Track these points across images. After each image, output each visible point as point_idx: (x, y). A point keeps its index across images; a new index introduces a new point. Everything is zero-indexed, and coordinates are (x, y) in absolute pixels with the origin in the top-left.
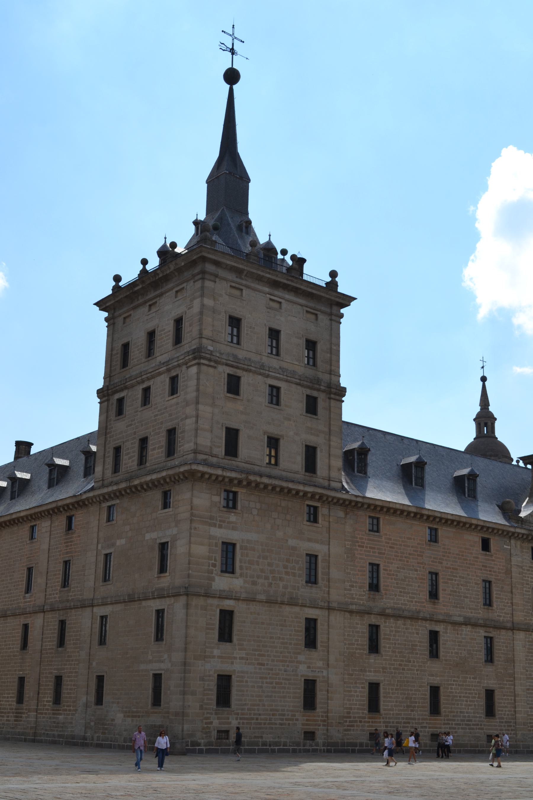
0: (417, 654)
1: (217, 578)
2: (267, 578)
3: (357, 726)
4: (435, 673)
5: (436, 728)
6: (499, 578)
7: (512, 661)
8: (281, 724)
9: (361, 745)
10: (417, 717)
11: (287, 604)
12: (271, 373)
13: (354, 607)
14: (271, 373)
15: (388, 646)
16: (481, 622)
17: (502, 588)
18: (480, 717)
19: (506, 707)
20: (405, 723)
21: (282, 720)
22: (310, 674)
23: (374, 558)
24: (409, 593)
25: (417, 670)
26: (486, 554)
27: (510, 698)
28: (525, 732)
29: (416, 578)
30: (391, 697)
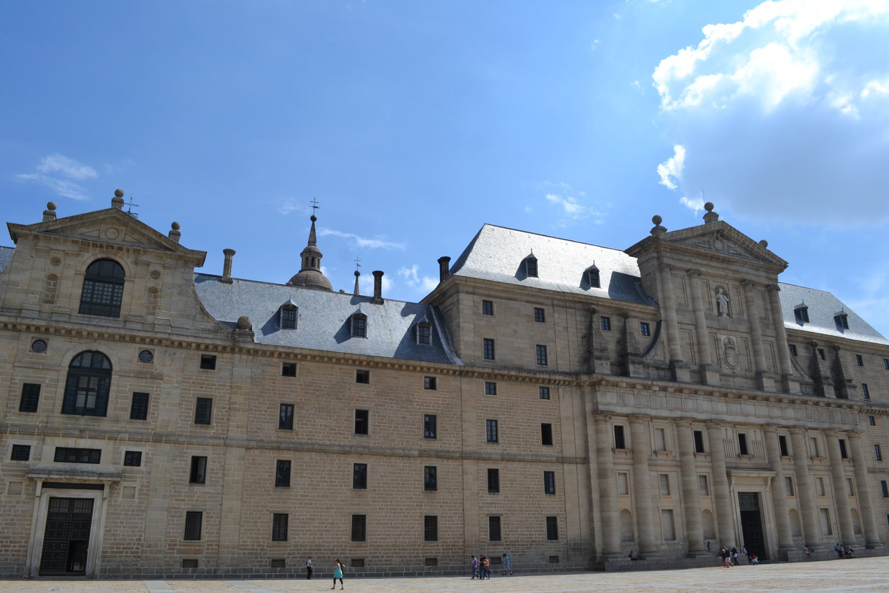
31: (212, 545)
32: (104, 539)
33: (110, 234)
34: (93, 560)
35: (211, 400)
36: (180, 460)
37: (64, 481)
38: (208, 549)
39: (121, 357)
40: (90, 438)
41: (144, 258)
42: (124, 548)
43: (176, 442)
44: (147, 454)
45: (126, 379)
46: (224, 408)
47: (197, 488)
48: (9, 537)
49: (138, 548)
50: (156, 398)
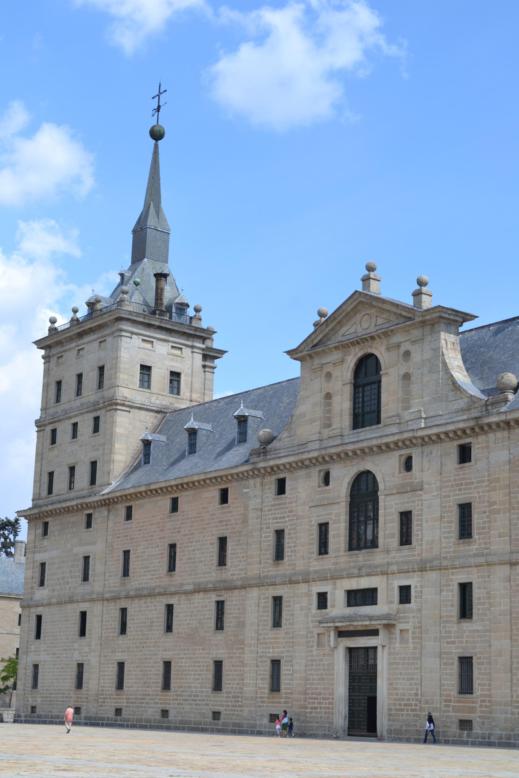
0: (154, 630)
1: (36, 591)
2: (60, 584)
3: (108, 702)
4: (167, 647)
5: (166, 704)
6: (236, 530)
7: (241, 625)
8: (62, 701)
9: (108, 719)
10: (151, 693)
11: (69, 603)
12: (71, 414)
13: (107, 595)
14: (71, 414)
15: (132, 626)
16: (210, 586)
17: (239, 540)
18: (207, 692)
19: (234, 679)
20: (141, 699)
21: (63, 697)
22: (81, 659)
23: (126, 545)
24: (150, 571)
25: (154, 647)
26: (223, 507)
27: (239, 669)
28: (252, 709)
29: (157, 555)
30: (132, 675)
31: (484, 701)
32: (389, 694)
33: (362, 325)
34: (382, 721)
35: (470, 504)
36: (447, 591)
37: (352, 629)
38: (481, 706)
39: (386, 470)
40: (367, 575)
41: (395, 339)
42: (405, 705)
43: (440, 568)
44: (416, 587)
45: (392, 497)
46: (485, 512)
47: (466, 625)
48: (320, 694)
49: (416, 705)
50: (418, 515)
